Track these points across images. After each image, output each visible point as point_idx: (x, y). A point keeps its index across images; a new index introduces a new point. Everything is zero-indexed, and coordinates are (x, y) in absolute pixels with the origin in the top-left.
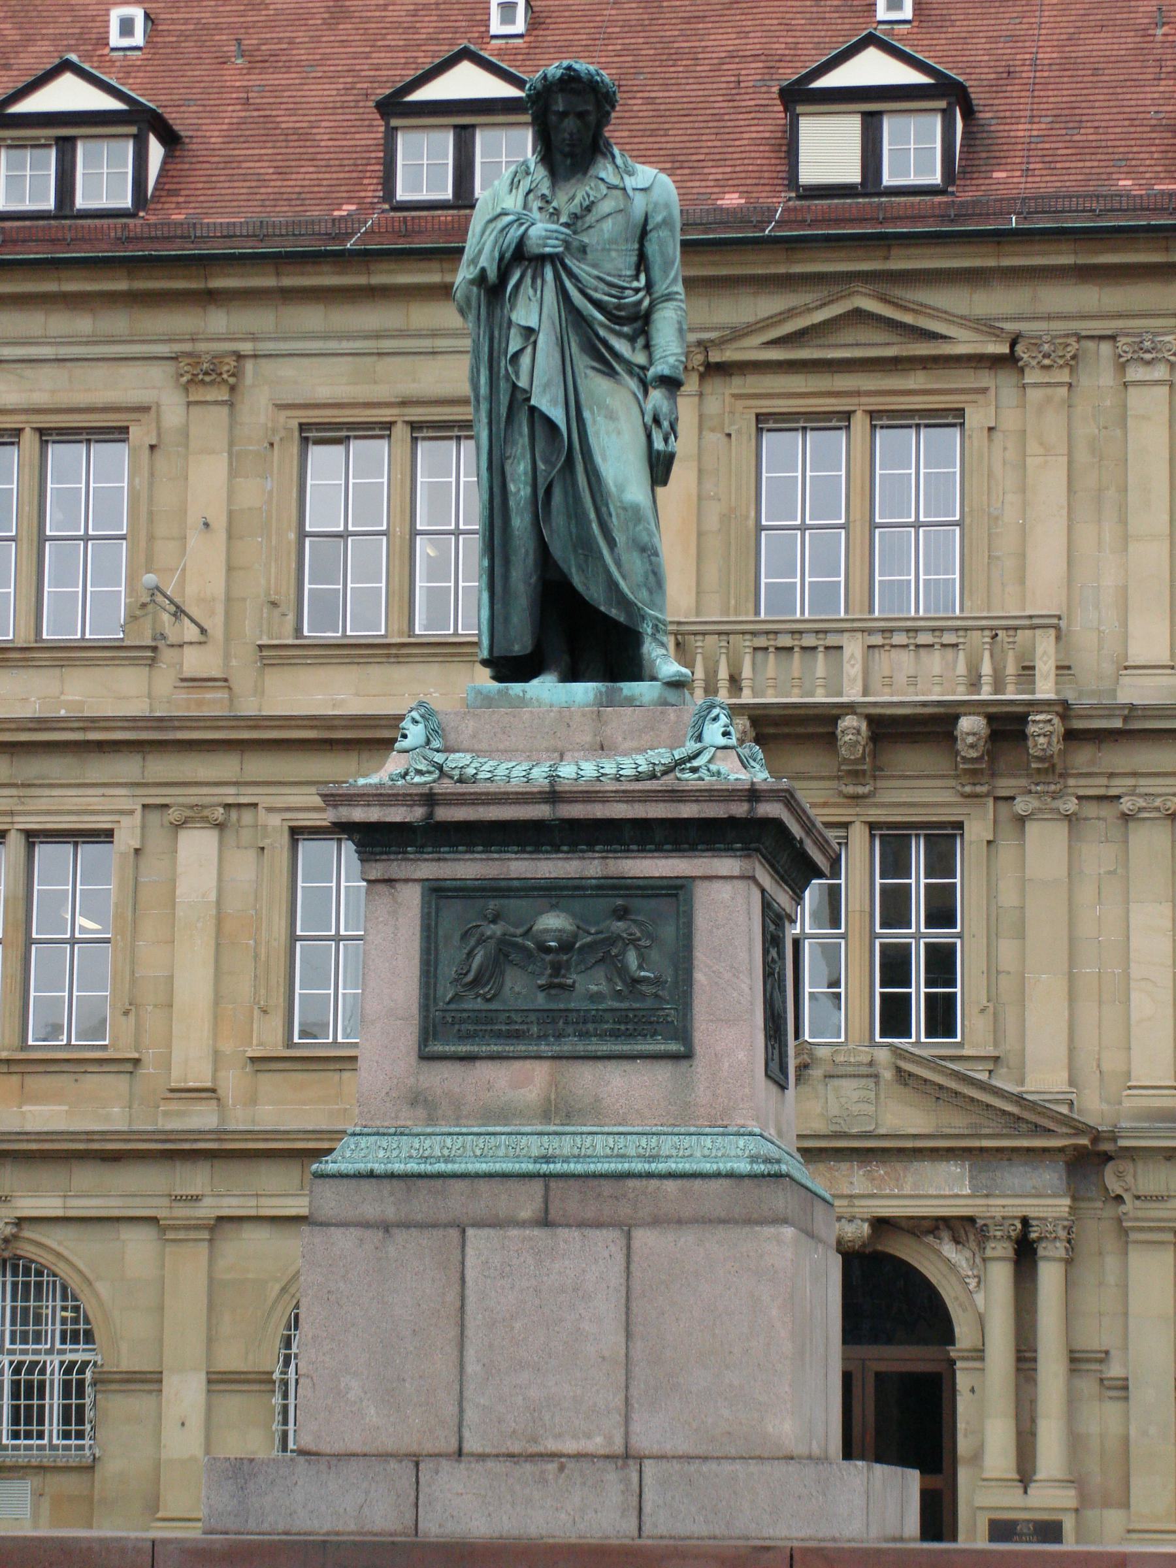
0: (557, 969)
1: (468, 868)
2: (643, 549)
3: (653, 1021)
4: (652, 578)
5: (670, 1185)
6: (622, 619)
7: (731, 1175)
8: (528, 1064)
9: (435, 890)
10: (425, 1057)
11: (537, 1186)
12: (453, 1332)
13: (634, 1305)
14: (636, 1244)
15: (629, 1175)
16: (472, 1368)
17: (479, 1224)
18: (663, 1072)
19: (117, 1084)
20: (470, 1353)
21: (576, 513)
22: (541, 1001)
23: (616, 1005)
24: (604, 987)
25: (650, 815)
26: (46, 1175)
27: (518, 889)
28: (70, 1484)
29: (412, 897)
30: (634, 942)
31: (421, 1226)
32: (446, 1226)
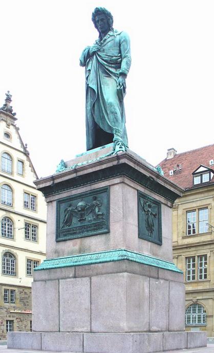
0: (82, 215)
1: (64, 195)
2: (113, 113)
3: (101, 226)
4: (115, 119)
5: (100, 265)
6: (110, 132)
7: (113, 261)
8: (76, 240)
9: (59, 201)
10: (58, 241)
11: (73, 268)
12: (58, 304)
13: (92, 295)
14: (92, 280)
15: (92, 264)
16: (61, 312)
17: (62, 279)
18: (103, 238)
19: (208, 283)
20: (61, 308)
21: (100, 111)
22: (79, 224)
23: (94, 222)
24: (92, 219)
25: (97, 170)
26: (200, 294)
27: (74, 198)
28: (204, 328)
29: (55, 204)
30: (97, 205)
31: (51, 280)
32: (55, 280)
